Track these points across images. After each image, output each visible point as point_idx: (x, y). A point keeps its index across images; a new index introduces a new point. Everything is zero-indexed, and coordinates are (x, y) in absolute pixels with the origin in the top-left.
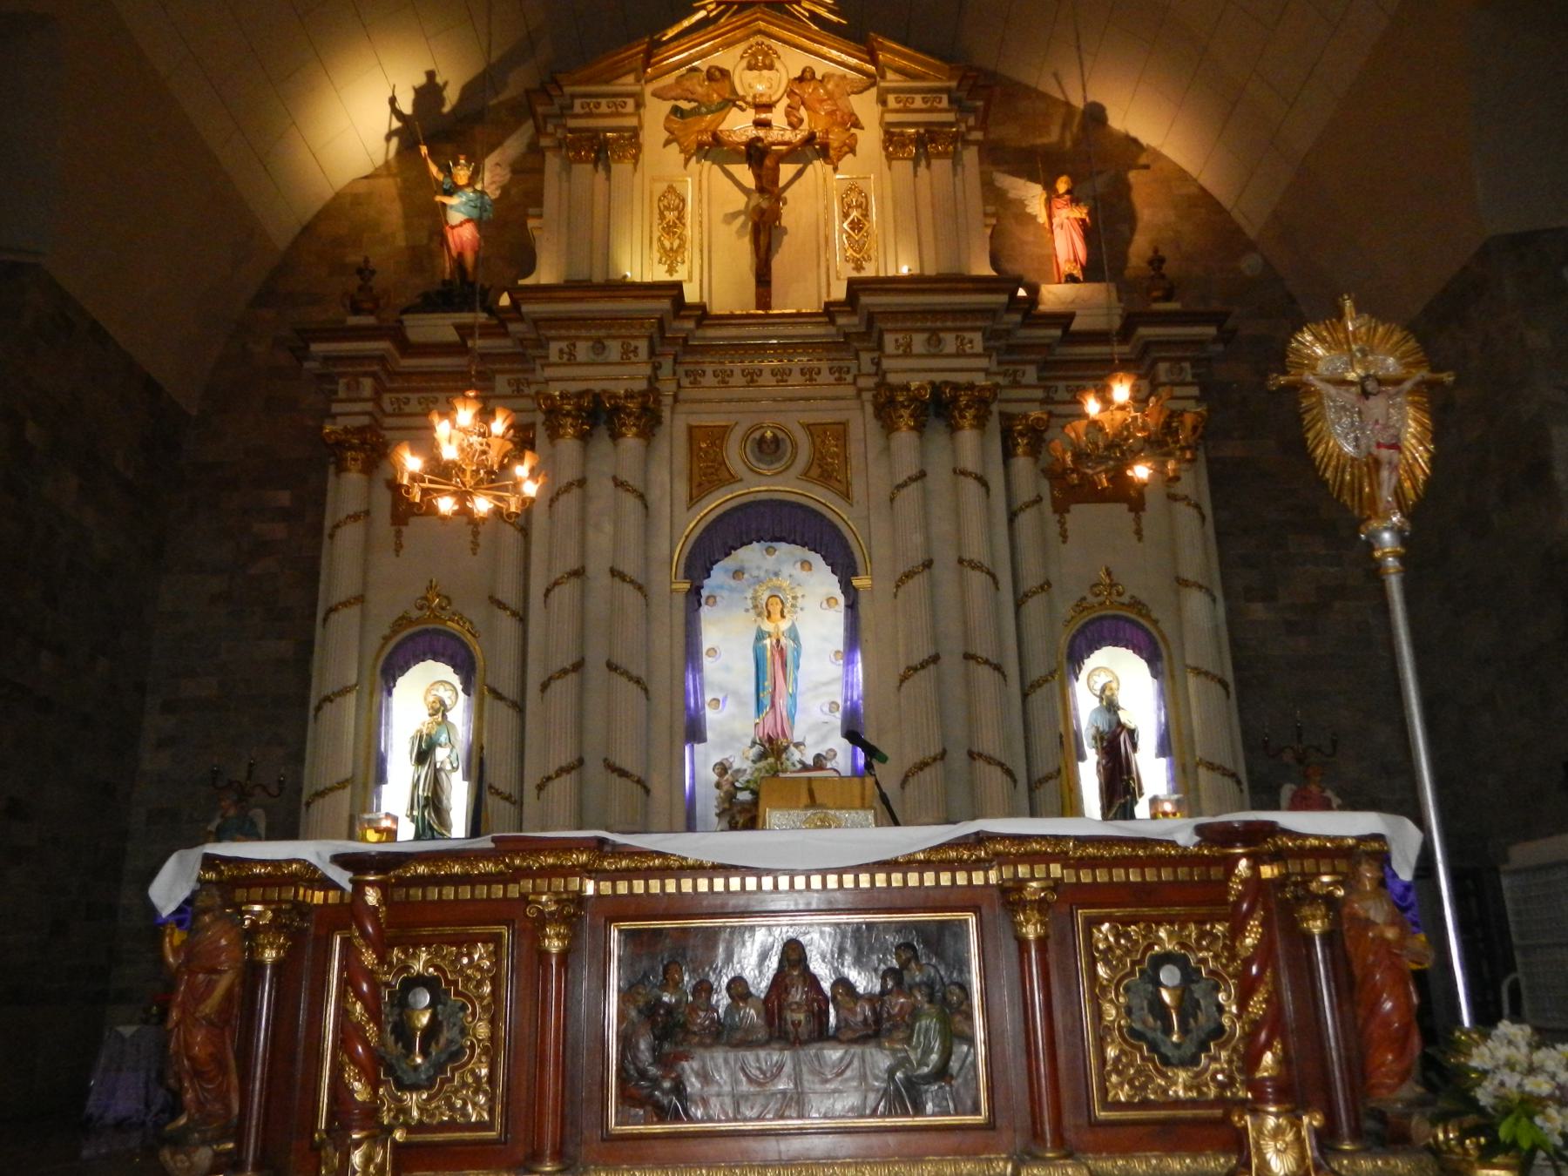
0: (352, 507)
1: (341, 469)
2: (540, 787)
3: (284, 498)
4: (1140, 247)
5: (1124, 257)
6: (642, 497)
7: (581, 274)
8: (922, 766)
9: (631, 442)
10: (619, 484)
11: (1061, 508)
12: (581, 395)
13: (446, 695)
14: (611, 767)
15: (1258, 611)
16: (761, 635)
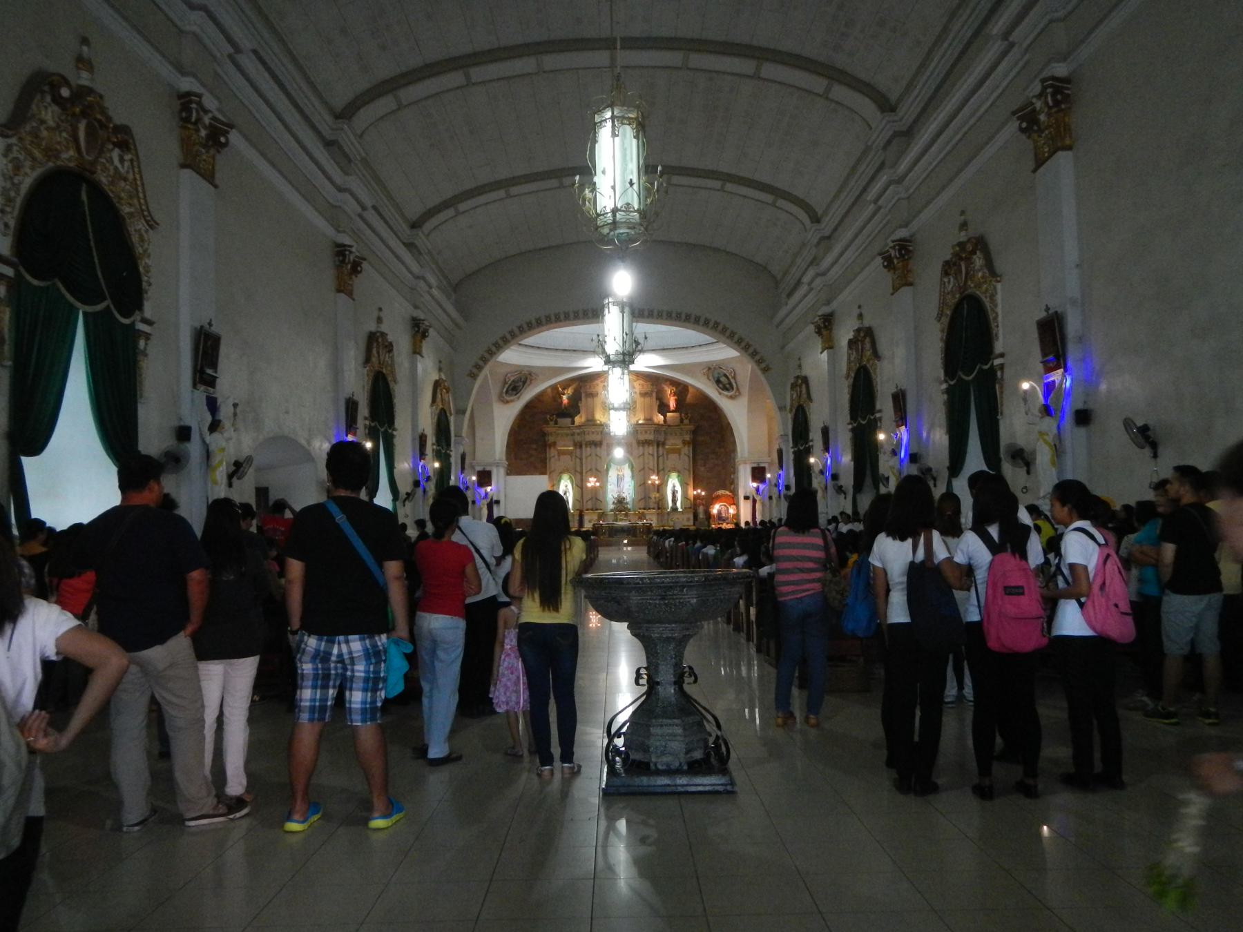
0: (552, 455)
1: (550, 448)
2: (587, 501)
3: (534, 446)
4: (689, 396)
5: (685, 399)
6: (600, 458)
7: (590, 418)
8: (642, 499)
9: (598, 449)
10: (597, 455)
11: (667, 455)
12: (590, 441)
13: (566, 483)
14: (597, 499)
15: (702, 469)
16: (618, 475)
